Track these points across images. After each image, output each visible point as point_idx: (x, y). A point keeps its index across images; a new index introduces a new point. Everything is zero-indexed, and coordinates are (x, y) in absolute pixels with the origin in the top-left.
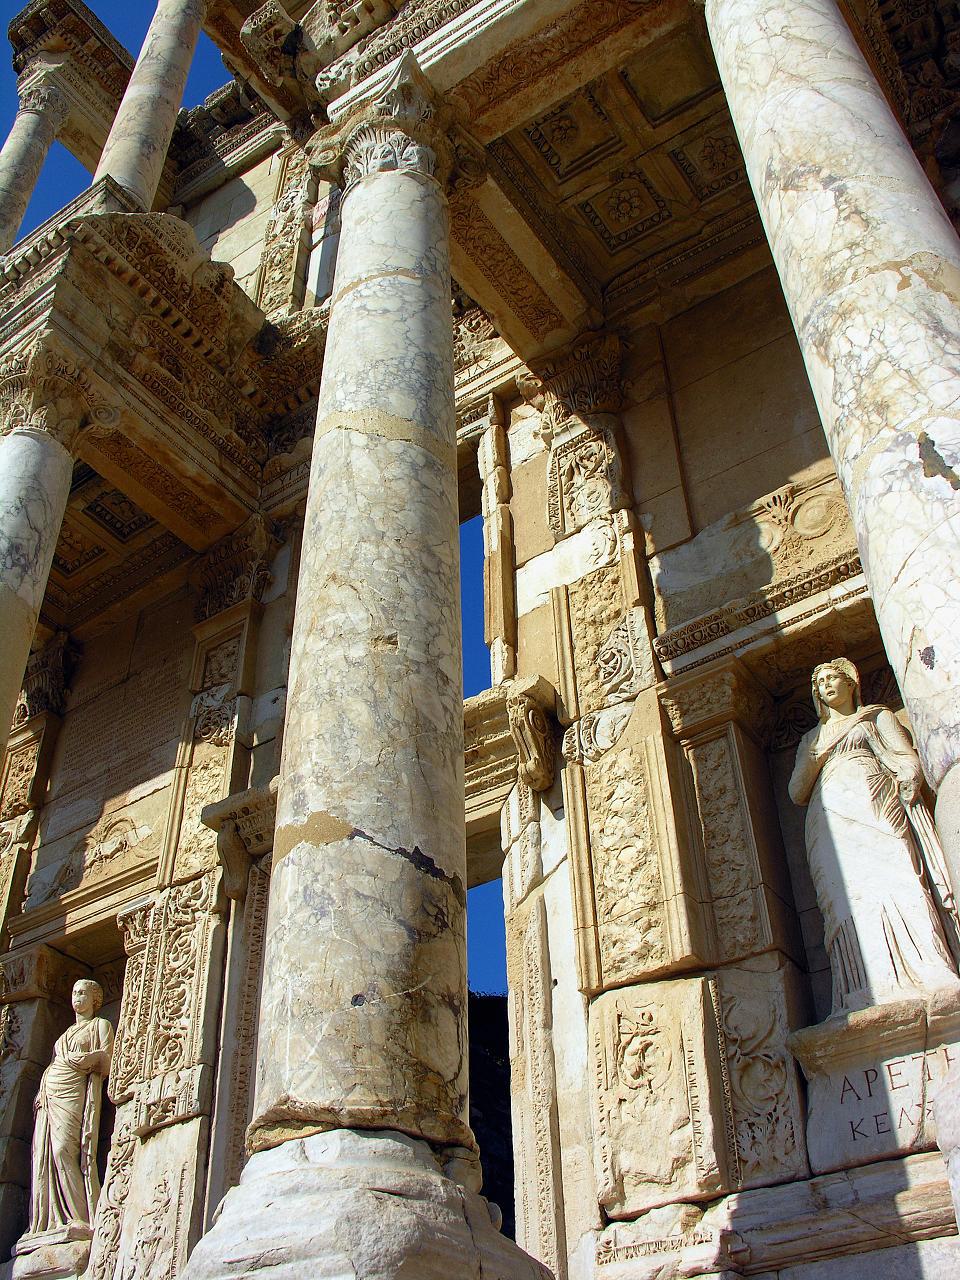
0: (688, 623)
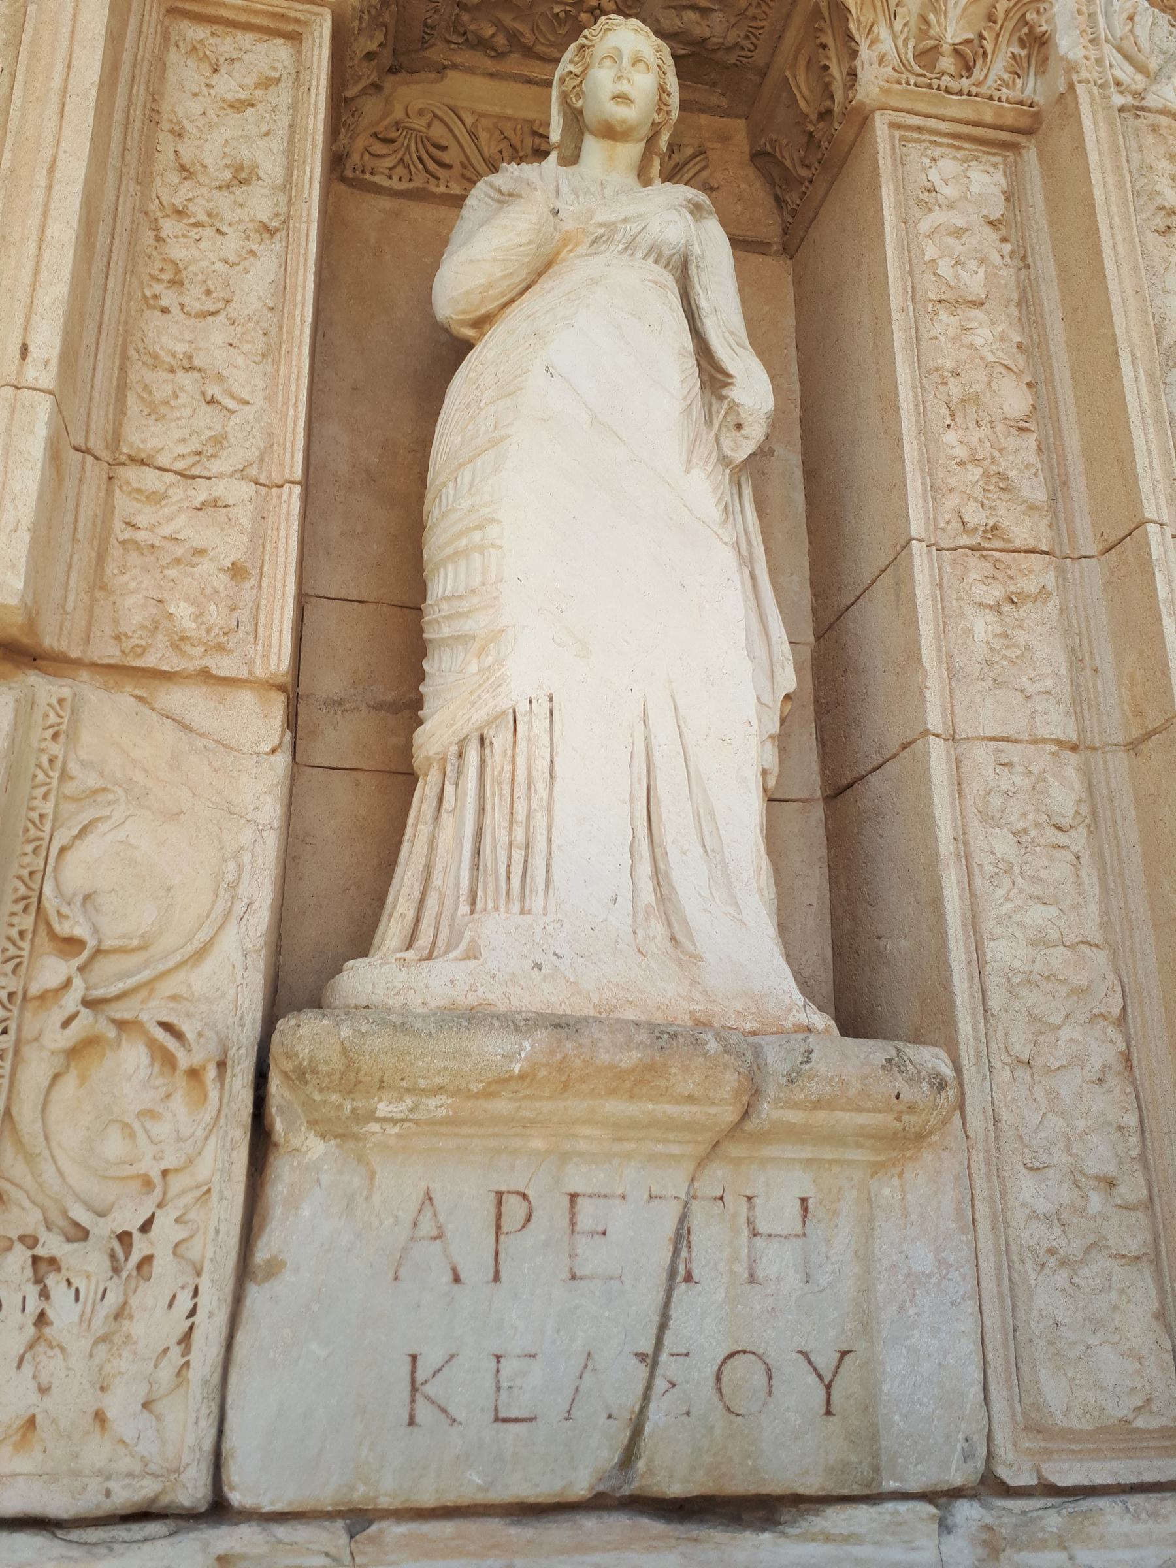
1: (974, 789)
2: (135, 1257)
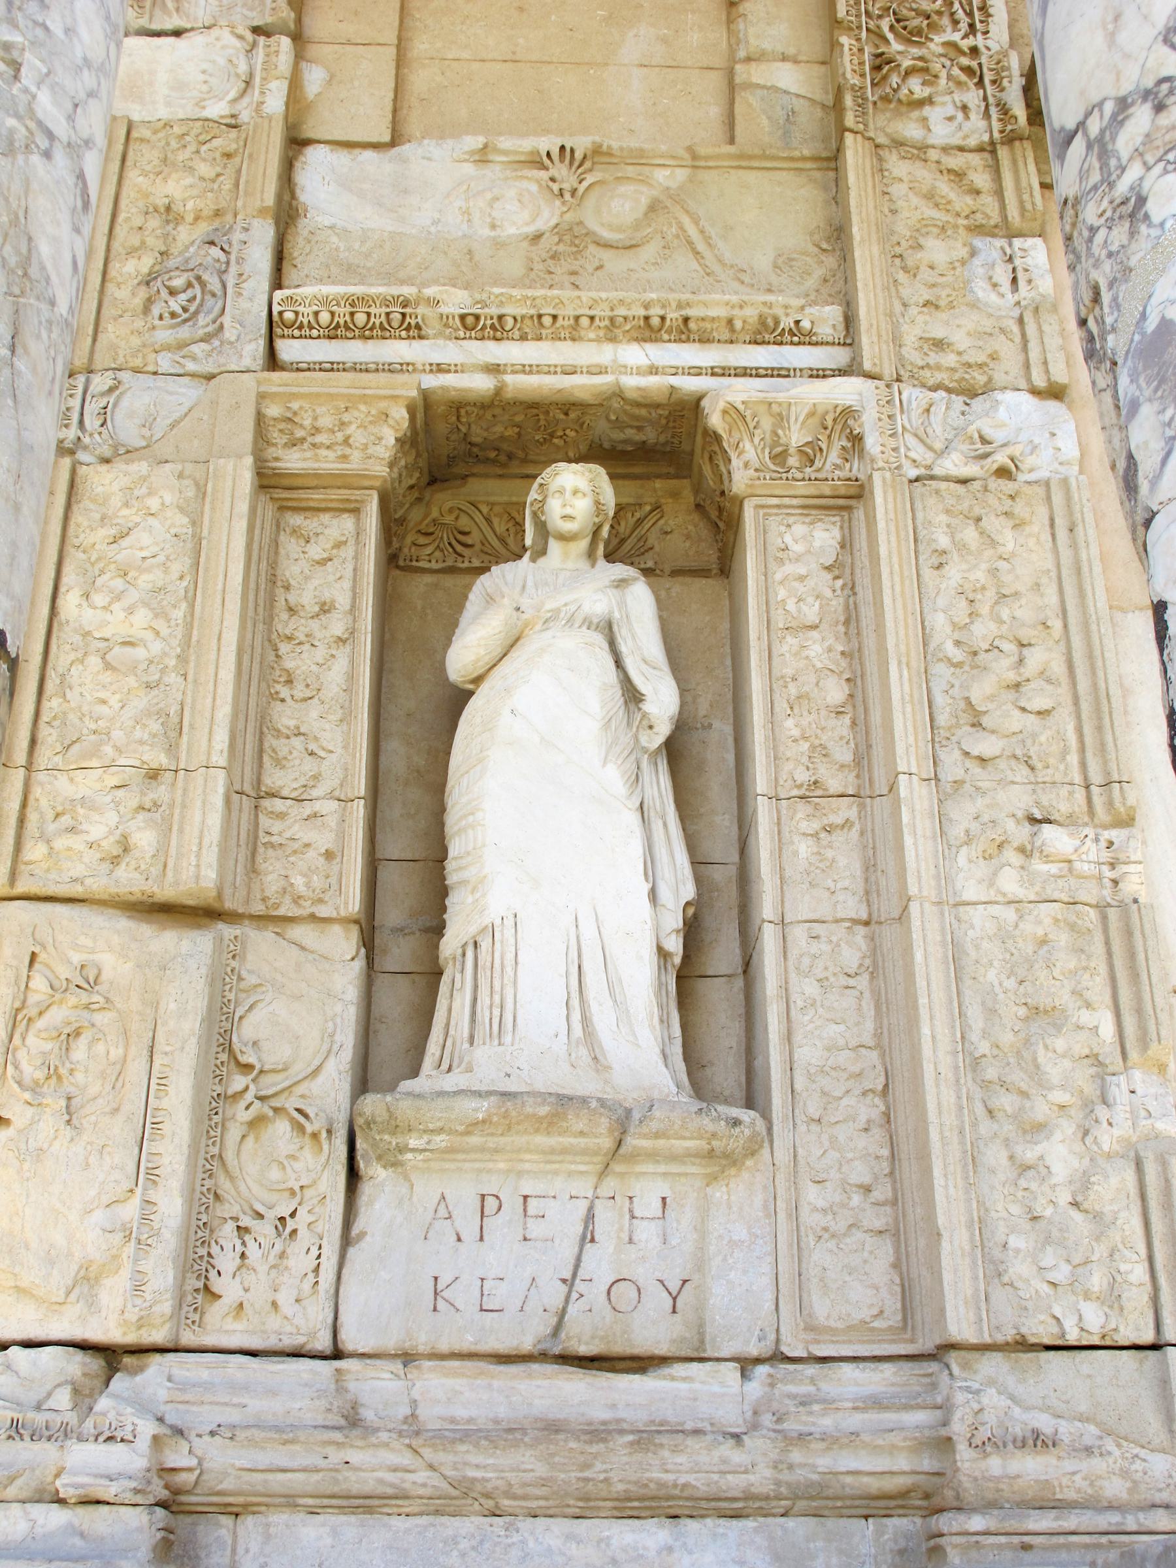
0: (352, 289)
1: (793, 953)
2: (288, 1230)
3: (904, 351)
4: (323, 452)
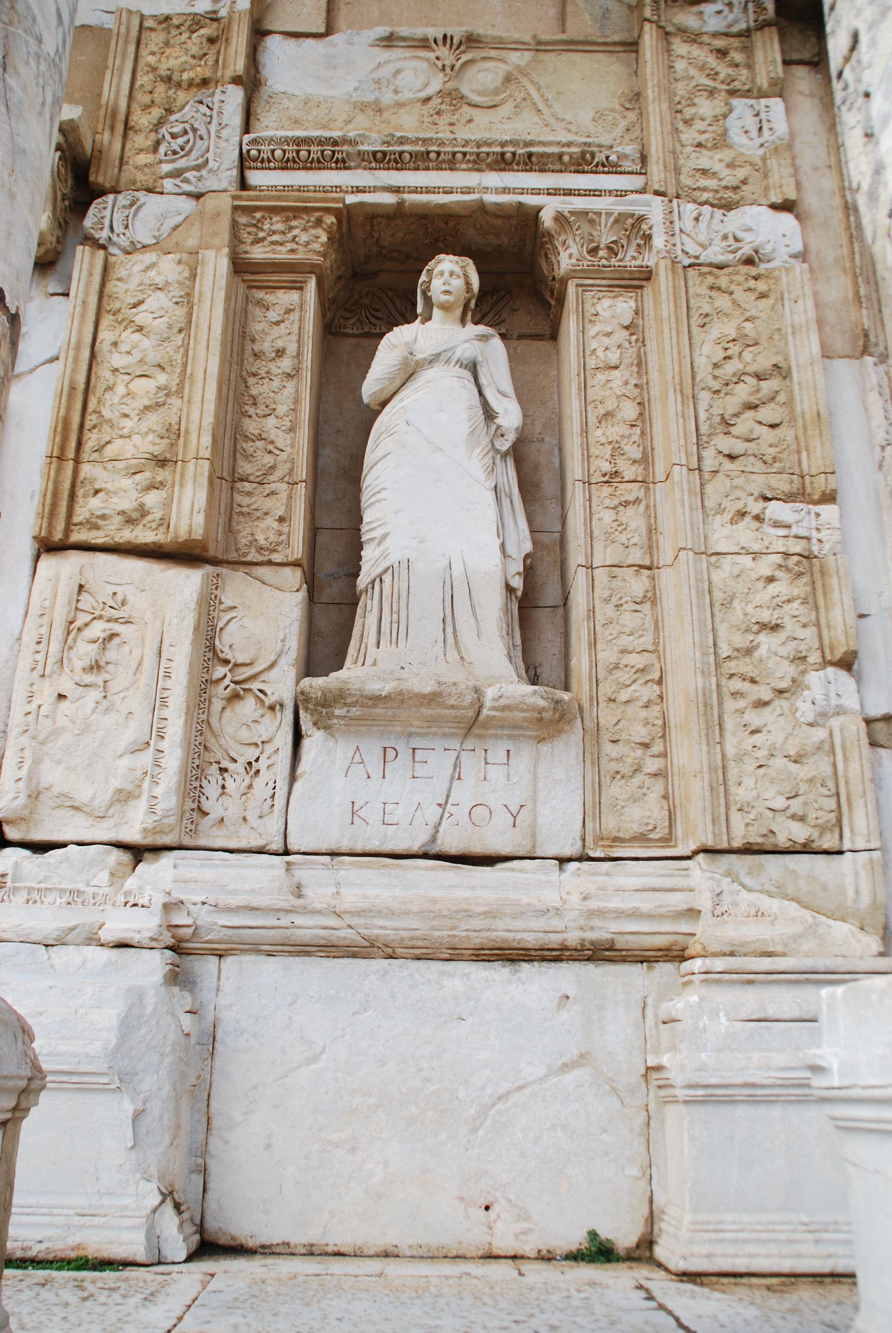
2: (253, 770)
3: (682, 177)
4: (279, 248)
